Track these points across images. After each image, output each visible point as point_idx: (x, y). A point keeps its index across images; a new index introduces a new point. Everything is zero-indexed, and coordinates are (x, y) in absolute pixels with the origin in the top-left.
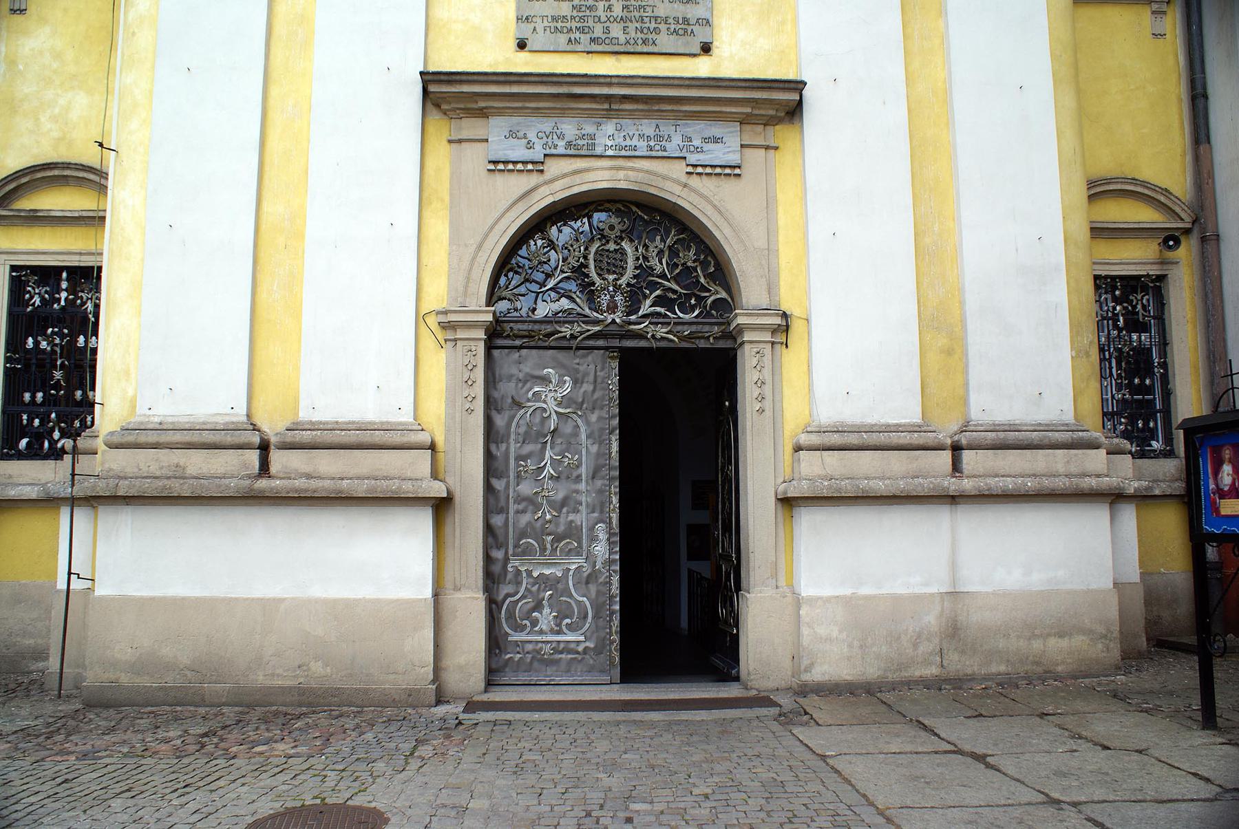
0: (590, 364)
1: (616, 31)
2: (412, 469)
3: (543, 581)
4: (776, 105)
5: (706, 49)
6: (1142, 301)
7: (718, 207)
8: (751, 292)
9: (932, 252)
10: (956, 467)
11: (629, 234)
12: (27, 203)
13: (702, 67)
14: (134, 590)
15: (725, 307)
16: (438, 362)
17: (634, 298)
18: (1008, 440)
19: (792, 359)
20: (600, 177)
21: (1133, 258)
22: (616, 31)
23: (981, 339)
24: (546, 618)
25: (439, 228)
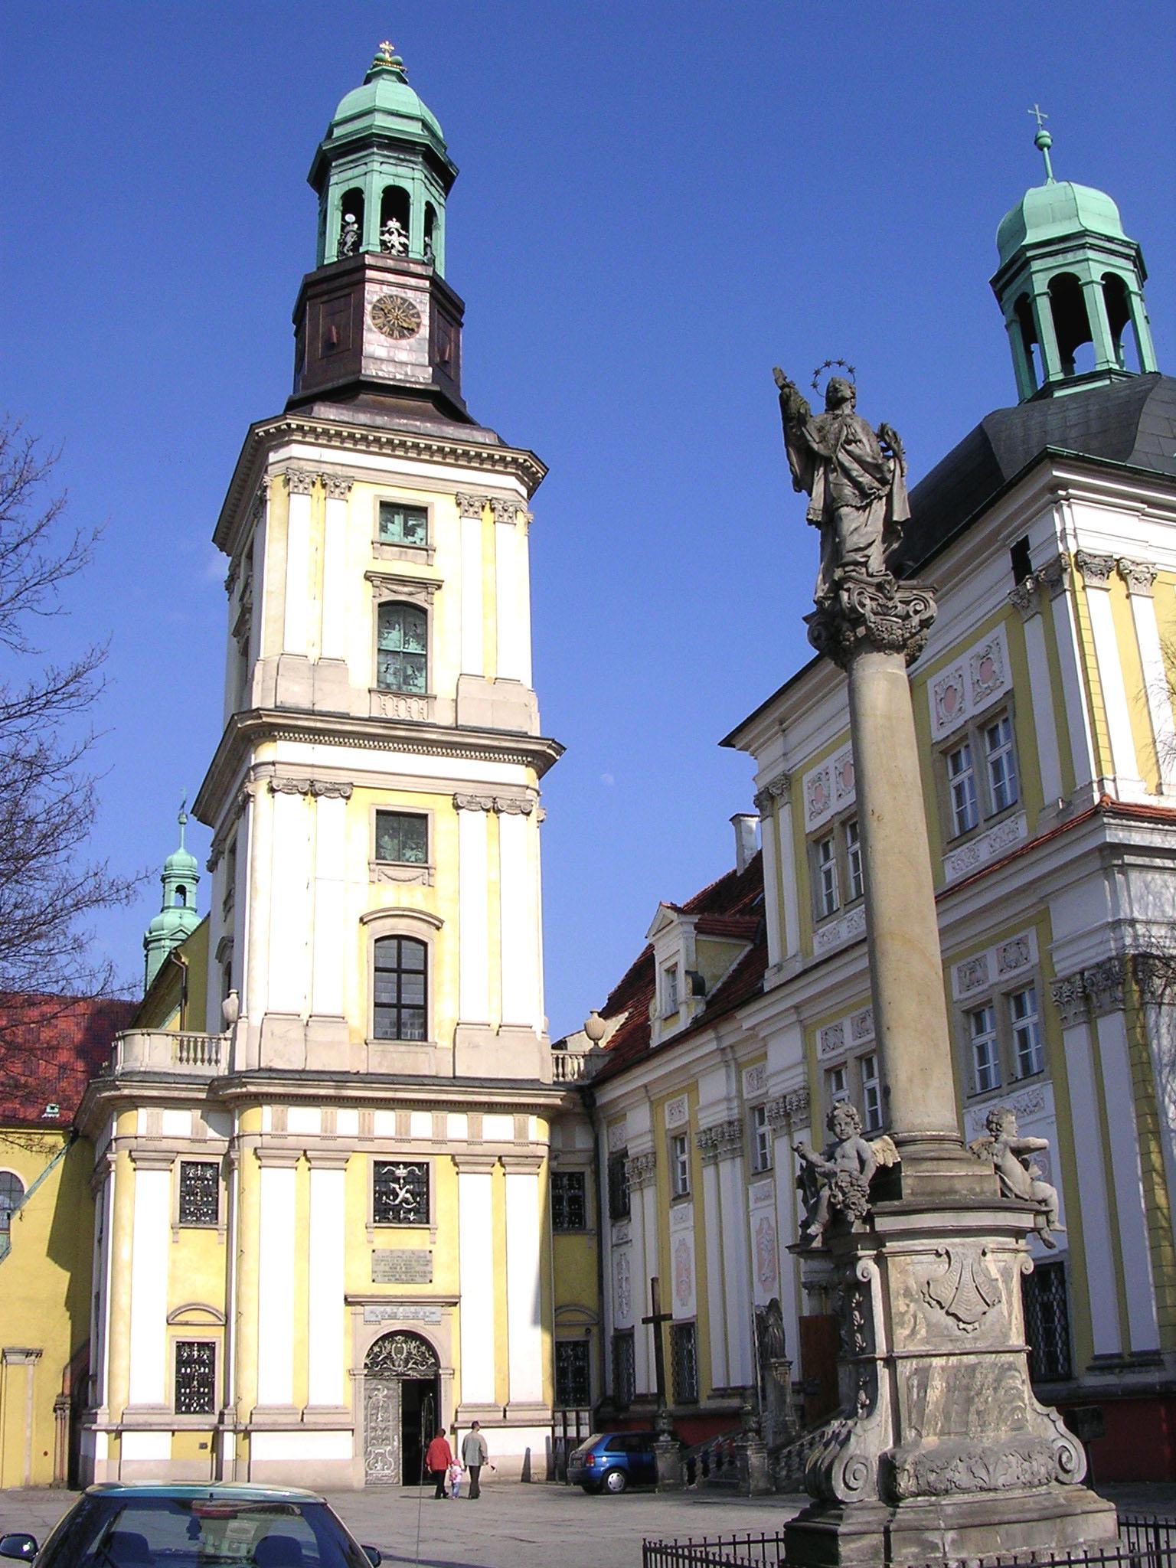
0: (392, 1385)
2: (346, 1419)
3: (381, 1454)
4: (453, 1302)
6: (580, 1349)
11: (406, 1342)
12: (180, 1318)
14: (265, 1457)
15: (437, 1364)
16: (350, 1385)
17: (407, 1362)
18: (521, 1406)
19: (455, 1383)
21: (576, 1335)
24: (379, 1465)
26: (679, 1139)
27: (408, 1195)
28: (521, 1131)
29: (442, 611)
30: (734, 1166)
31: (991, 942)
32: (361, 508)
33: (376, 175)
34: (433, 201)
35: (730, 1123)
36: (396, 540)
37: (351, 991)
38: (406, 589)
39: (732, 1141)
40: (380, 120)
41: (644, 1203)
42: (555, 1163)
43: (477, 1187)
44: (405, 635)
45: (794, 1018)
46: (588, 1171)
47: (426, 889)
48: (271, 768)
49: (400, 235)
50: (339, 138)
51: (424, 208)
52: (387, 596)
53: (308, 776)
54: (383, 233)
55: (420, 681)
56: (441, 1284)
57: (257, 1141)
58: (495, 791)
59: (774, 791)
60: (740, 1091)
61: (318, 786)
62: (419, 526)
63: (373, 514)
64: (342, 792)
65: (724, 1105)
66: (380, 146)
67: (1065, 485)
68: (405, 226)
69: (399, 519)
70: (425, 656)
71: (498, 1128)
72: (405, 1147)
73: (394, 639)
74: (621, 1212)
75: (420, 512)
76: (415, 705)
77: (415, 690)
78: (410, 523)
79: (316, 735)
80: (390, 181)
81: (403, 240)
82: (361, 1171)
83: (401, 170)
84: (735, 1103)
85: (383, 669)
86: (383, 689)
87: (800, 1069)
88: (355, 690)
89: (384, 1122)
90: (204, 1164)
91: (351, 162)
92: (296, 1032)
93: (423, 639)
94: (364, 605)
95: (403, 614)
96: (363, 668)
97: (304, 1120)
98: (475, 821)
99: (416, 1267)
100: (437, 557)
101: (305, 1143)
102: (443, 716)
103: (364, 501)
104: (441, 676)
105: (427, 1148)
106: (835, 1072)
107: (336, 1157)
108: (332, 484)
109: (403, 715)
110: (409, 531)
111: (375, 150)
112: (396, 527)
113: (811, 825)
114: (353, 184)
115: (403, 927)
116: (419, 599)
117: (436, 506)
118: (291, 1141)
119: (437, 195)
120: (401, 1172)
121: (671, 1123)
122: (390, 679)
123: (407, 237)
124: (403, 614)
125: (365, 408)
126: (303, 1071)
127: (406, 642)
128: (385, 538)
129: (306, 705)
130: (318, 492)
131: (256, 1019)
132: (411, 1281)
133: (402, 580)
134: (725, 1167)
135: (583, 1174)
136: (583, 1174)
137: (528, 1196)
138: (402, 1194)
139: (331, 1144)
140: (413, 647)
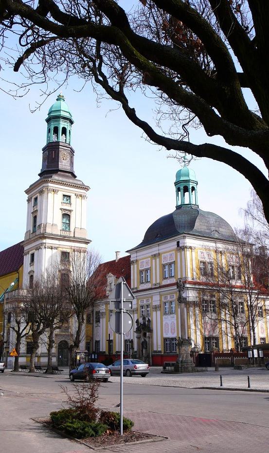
31: (169, 294)
32: (60, 195)
36: (65, 202)
52: (64, 213)
63: (62, 197)
66: (62, 118)
67: (185, 236)
73: (64, 220)
75: (70, 197)
79: (53, 238)
80: (63, 126)
83: (66, 124)
88: (57, 231)
93: (69, 221)
94: (59, 214)
95: (67, 216)
100: (72, 205)
102: (72, 235)
104: (72, 229)
106: (142, 307)
110: (67, 200)
112: (65, 199)
114: (56, 126)
116: (69, 213)
124: (67, 216)
125: (60, 175)
128: (63, 201)
129: (51, 233)
133: (66, 210)
140: (68, 222)
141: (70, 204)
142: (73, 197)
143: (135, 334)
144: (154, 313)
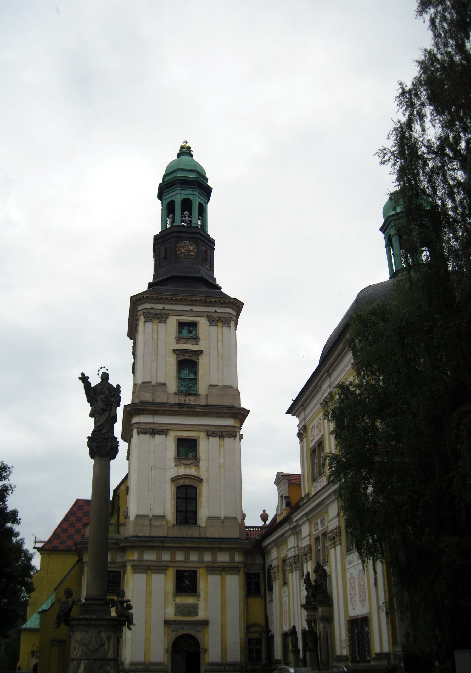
1: (187, 613)
4: (205, 623)
5: (197, 615)
7: (199, 636)
8: (202, 646)
9: (223, 641)
10: (225, 668)
13: (196, 618)
15: (199, 647)
20: (184, 632)
22: (187, 613)
23: (229, 652)
25: (166, 639)
26: (284, 561)
27: (189, 583)
28: (232, 558)
29: (202, 361)
30: (292, 574)
33: (179, 195)
34: (202, 202)
35: (295, 556)
36: (185, 336)
37: (167, 506)
38: (188, 355)
39: (296, 563)
40: (180, 174)
41: (276, 585)
42: (246, 570)
43: (214, 579)
44: (189, 371)
45: (305, 519)
46: (261, 572)
47: (196, 467)
48: (138, 425)
49: (189, 217)
50: (168, 180)
51: (197, 205)
52: (181, 358)
53: (151, 427)
54: (182, 217)
55: (194, 389)
56: (201, 615)
57: (133, 563)
58: (223, 429)
59: (302, 432)
60: (298, 544)
61: (155, 431)
62: (194, 330)
64: (163, 431)
65: (293, 550)
66: (180, 184)
68: (191, 213)
69: (186, 328)
70: (196, 379)
71: (224, 558)
72: (188, 565)
73: (185, 373)
74: (271, 589)
75: (194, 325)
76: (192, 398)
77: (192, 392)
78: (190, 329)
79: (154, 413)
80: (184, 197)
81: (189, 219)
82: (171, 573)
83: (188, 192)
84: (296, 549)
85: (180, 385)
86: (179, 393)
87: (308, 538)
89: (180, 557)
90: (115, 572)
91: (170, 190)
92: (146, 522)
93: (195, 373)
94: (172, 361)
96: (172, 386)
97: (149, 556)
98: (215, 441)
99: (193, 610)
101: (150, 563)
102: (202, 402)
103: (173, 321)
105: (196, 565)
107: (160, 568)
108: (161, 317)
109: (187, 402)
110: (190, 332)
111: (179, 185)
112: (185, 332)
113: (311, 445)
114: (170, 200)
115: (187, 482)
116: (194, 358)
117: (200, 322)
118: (145, 563)
119: (204, 199)
120: (186, 574)
121: (282, 555)
122: (183, 388)
123: (191, 218)
126: (149, 537)
127: (189, 374)
128: (181, 335)
129: (150, 400)
130: (156, 321)
131: (132, 517)
132: (190, 615)
134: (294, 573)
135: (259, 573)
136: (259, 573)
137: (234, 583)
138: (186, 582)
139: (159, 564)
140: (192, 376)
141: (196, 339)
142: (203, 323)
143: (305, 612)
144: (332, 552)
